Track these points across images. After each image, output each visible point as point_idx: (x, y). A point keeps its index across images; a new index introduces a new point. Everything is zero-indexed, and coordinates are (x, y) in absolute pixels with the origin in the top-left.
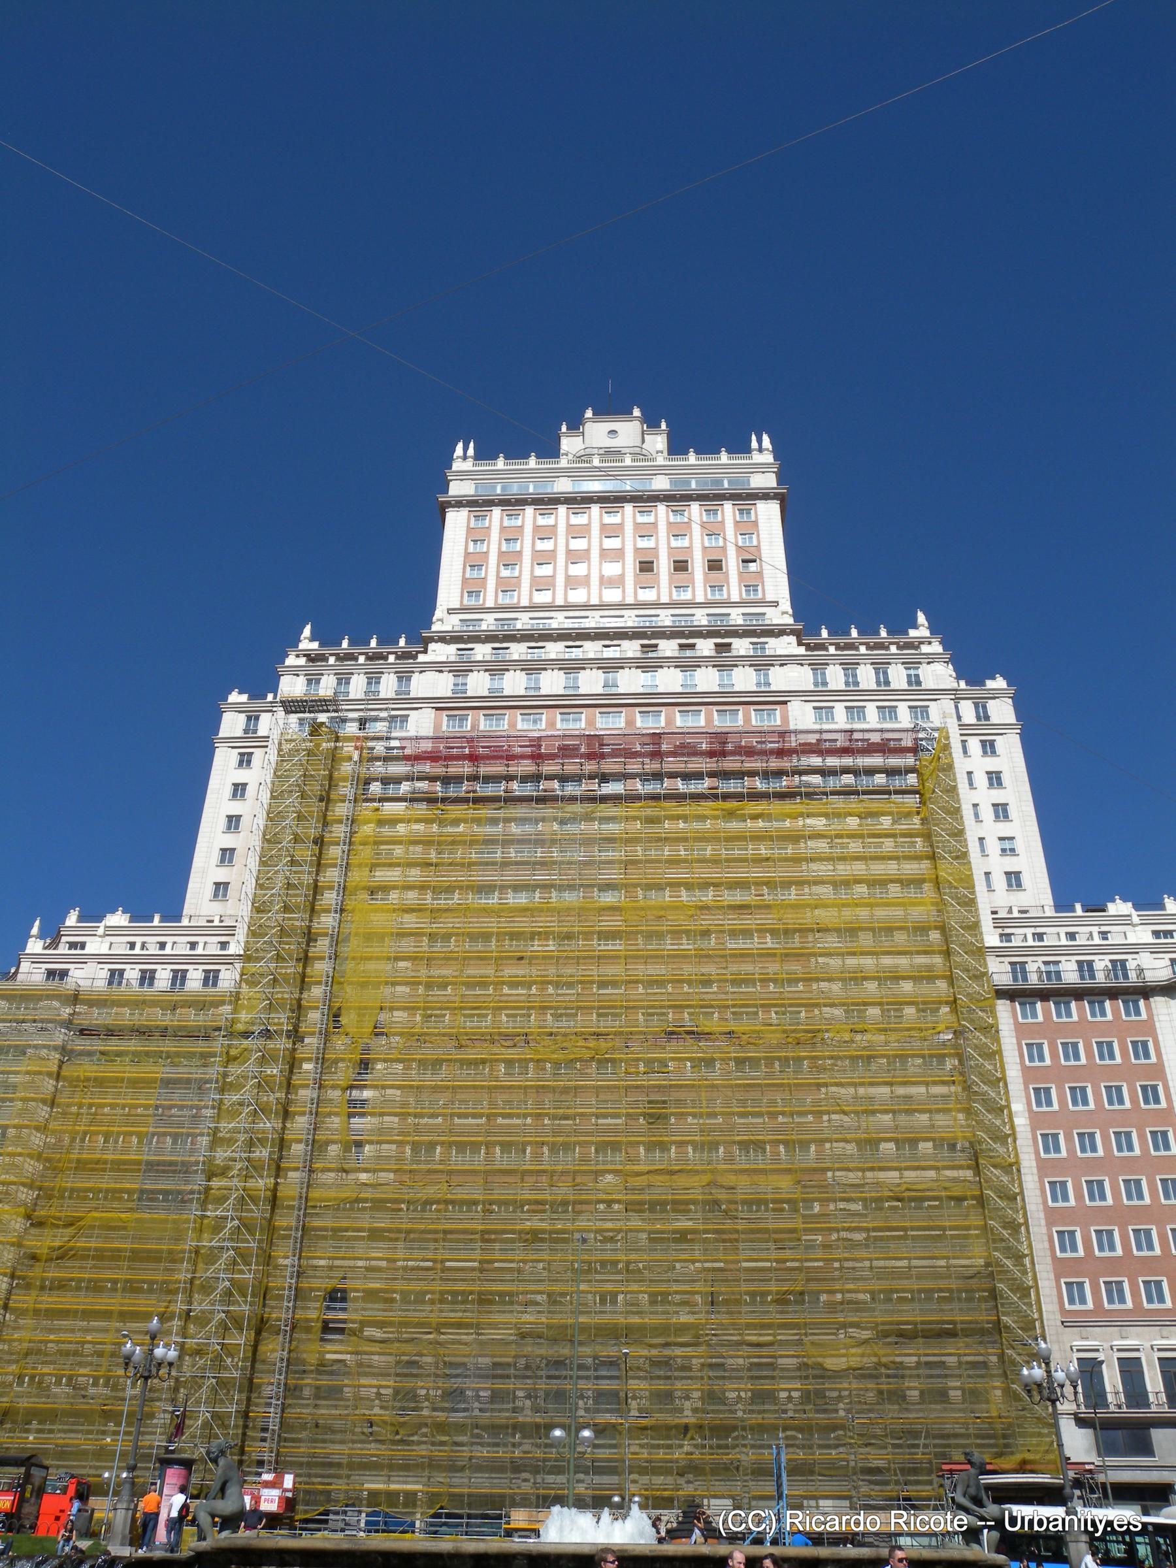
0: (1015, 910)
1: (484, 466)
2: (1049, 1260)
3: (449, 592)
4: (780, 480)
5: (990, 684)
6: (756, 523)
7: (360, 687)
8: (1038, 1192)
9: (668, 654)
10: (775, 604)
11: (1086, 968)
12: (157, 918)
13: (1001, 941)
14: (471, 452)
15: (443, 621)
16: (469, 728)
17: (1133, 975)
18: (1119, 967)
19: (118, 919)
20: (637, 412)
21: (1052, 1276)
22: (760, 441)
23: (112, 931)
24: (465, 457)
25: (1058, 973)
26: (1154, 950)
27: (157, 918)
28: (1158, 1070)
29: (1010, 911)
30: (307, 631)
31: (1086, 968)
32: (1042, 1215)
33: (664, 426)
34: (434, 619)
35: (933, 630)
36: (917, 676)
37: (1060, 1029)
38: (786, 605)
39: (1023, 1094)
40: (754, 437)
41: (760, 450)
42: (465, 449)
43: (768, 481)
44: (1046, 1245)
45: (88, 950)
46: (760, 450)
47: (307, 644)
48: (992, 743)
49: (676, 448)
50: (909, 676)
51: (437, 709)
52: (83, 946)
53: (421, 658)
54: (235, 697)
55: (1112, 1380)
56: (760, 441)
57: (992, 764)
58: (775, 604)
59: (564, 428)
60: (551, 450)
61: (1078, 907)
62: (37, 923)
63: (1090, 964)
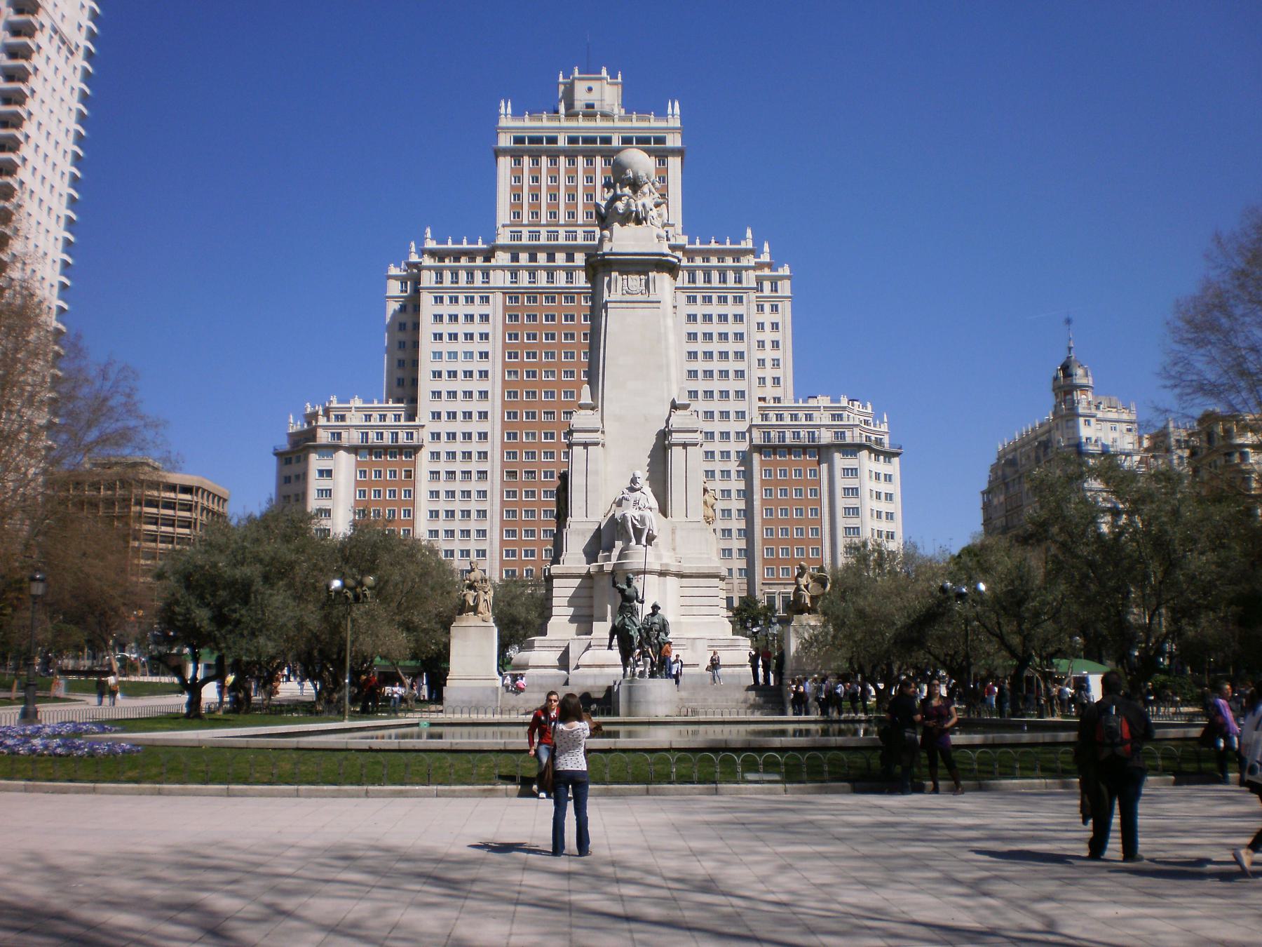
2: (761, 559)
3: (503, 214)
5: (781, 272)
10: (673, 225)
11: (797, 435)
12: (376, 402)
15: (504, 238)
17: (817, 440)
18: (812, 436)
19: (357, 403)
23: (358, 409)
26: (828, 427)
27: (376, 402)
31: (797, 435)
32: (760, 542)
33: (619, 75)
37: (779, 463)
38: (679, 230)
41: (673, 115)
43: (674, 141)
44: (761, 553)
45: (348, 423)
48: (777, 306)
50: (735, 278)
51: (503, 293)
52: (343, 418)
53: (493, 262)
54: (394, 271)
57: (775, 318)
58: (673, 225)
59: (561, 79)
63: (799, 433)
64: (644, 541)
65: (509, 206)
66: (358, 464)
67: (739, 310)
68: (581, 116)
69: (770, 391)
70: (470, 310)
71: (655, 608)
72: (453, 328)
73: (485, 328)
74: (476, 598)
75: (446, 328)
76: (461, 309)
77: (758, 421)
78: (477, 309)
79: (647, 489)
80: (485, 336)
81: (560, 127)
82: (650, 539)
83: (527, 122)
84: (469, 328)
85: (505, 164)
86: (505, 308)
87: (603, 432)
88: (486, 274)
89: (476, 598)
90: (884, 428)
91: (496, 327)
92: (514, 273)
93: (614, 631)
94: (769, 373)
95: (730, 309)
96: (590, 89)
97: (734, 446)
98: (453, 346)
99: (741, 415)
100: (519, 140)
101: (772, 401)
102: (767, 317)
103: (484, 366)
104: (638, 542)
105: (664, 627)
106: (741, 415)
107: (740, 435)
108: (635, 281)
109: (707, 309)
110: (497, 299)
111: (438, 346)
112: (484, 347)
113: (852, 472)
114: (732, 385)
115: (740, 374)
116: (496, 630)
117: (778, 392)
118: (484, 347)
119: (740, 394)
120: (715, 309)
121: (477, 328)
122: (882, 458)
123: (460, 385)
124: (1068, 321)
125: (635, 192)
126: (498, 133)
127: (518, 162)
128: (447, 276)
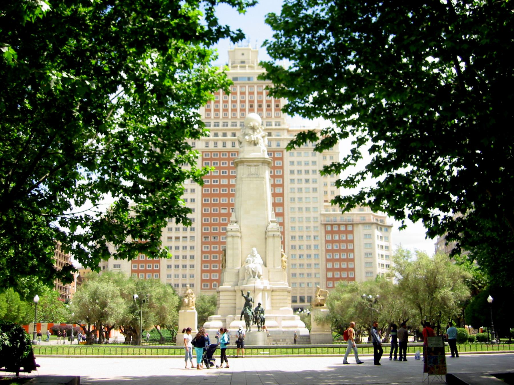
64: (256, 277)
68: (239, 67)
71: (259, 304)
74: (189, 301)
77: (324, 212)
79: (258, 256)
82: (259, 277)
87: (241, 232)
89: (189, 301)
93: (242, 313)
96: (243, 54)
97: (312, 224)
104: (254, 277)
105: (262, 312)
107: (315, 218)
108: (253, 170)
116: (196, 313)
122: (383, 229)
125: (254, 132)
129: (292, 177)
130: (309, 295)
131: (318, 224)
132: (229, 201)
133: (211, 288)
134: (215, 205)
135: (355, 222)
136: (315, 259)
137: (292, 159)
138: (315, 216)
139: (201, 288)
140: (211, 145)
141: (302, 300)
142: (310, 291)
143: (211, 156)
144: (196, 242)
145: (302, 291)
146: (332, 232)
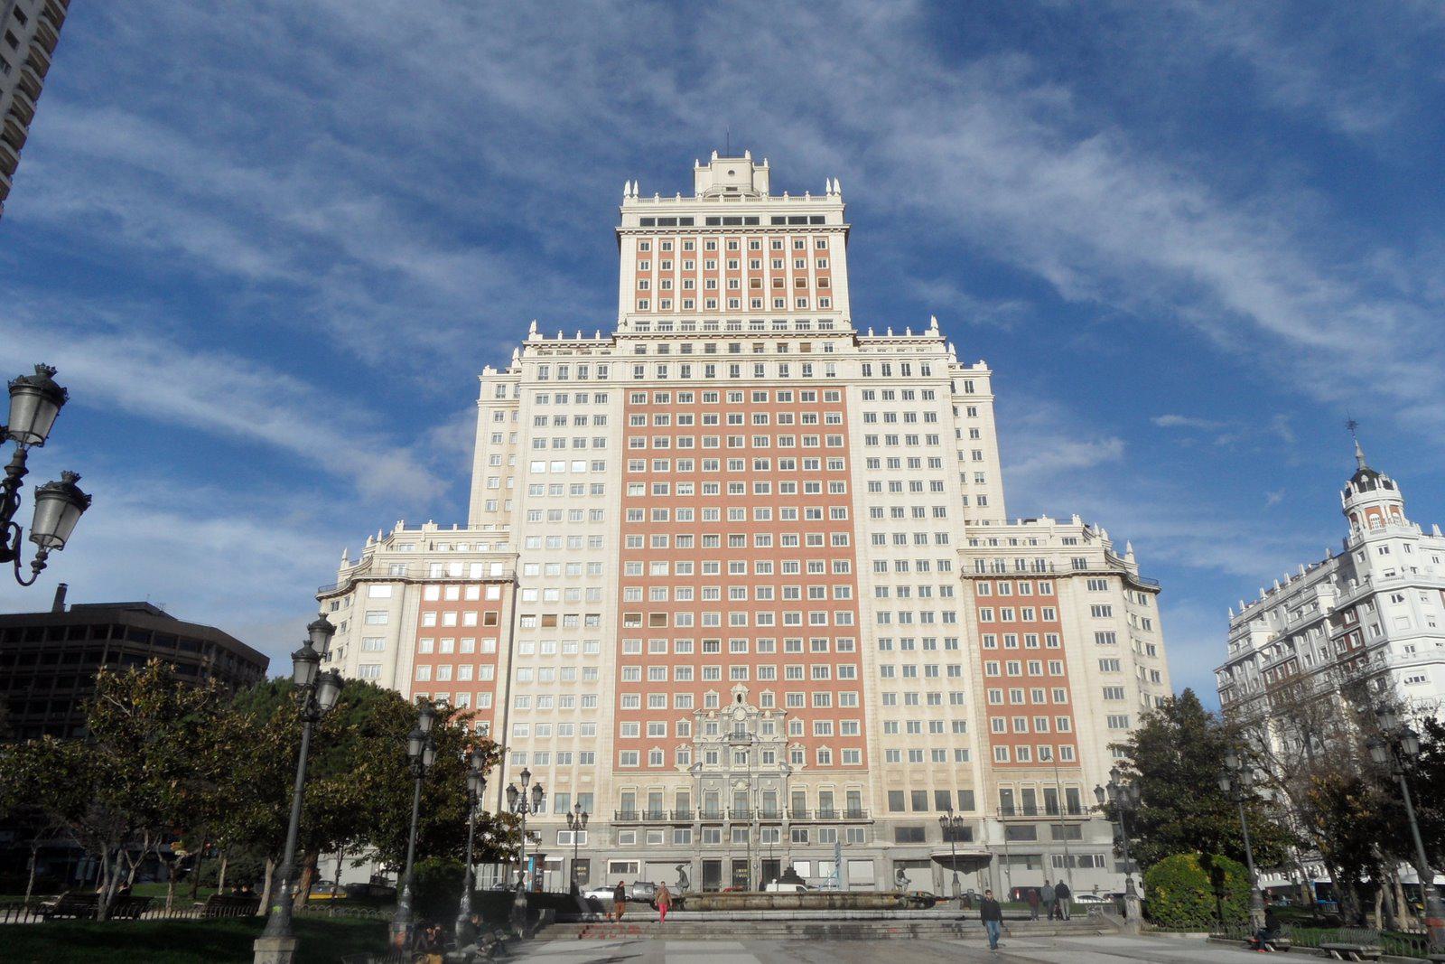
0: (980, 522)
1: (646, 204)
2: (988, 735)
4: (845, 221)
6: (828, 251)
7: (575, 373)
8: (983, 696)
9: (771, 352)
12: (455, 526)
13: (971, 545)
14: (636, 191)
16: (646, 403)
17: (1048, 568)
20: (748, 155)
21: (988, 744)
22: (832, 186)
24: (632, 195)
25: (1003, 566)
27: (455, 526)
28: (1057, 627)
29: (977, 524)
30: (533, 326)
32: (985, 709)
33: (766, 163)
34: (621, 319)
35: (942, 331)
36: (928, 368)
38: (847, 315)
39: (978, 639)
40: (828, 182)
42: (632, 188)
43: (835, 218)
44: (987, 726)
46: (833, 193)
47: (535, 338)
49: (776, 191)
50: (923, 368)
54: (488, 372)
55: (1018, 801)
56: (832, 186)
60: (688, 191)
61: (1019, 521)
62: (380, 533)
65: (634, 293)
66: (425, 606)
67: (929, 406)
69: (975, 512)
70: (581, 410)
72: (560, 432)
73: (600, 432)
75: (550, 432)
76: (571, 410)
78: (590, 409)
80: (599, 443)
81: (697, 208)
83: (659, 206)
84: (580, 432)
85: (629, 246)
86: (628, 409)
88: (603, 371)
90: (1130, 559)
91: (613, 432)
92: (639, 371)
94: (973, 491)
95: (919, 406)
96: (731, 172)
98: (559, 453)
99: (942, 538)
100: (647, 222)
101: (980, 522)
102: (965, 423)
103: (598, 478)
106: (942, 538)
107: (944, 565)
109: (889, 406)
110: (616, 399)
111: (539, 452)
112: (598, 455)
113: (1101, 611)
114: (928, 500)
115: (937, 486)
117: (985, 513)
118: (598, 455)
119: (939, 512)
120: (899, 406)
121: (589, 432)
123: (565, 503)
124: (1352, 425)
126: (621, 215)
127: (645, 246)
128: (553, 372)
129: (873, 452)
130: (941, 788)
131: (953, 579)
132: (698, 515)
133: (644, 768)
134: (657, 528)
135: (1059, 569)
136: (951, 682)
137: (870, 406)
138: (944, 557)
139: (616, 768)
140: (650, 372)
141: (919, 804)
142: (941, 776)
143: (650, 402)
144: (603, 630)
145: (917, 777)
146: (995, 601)
